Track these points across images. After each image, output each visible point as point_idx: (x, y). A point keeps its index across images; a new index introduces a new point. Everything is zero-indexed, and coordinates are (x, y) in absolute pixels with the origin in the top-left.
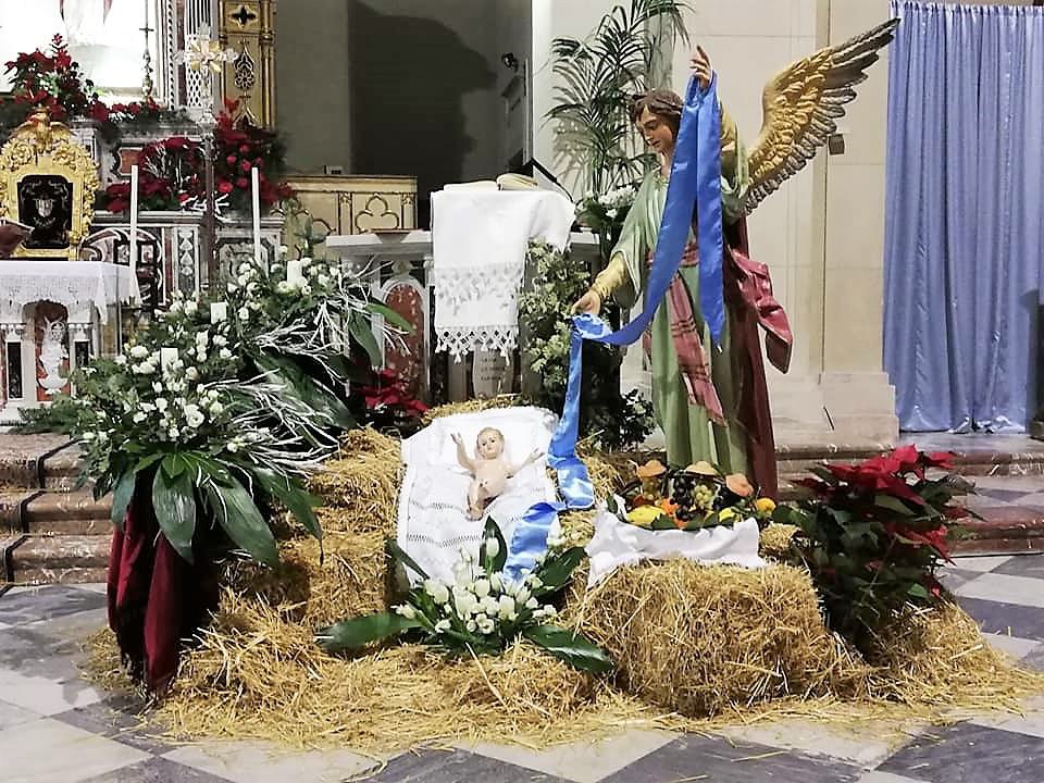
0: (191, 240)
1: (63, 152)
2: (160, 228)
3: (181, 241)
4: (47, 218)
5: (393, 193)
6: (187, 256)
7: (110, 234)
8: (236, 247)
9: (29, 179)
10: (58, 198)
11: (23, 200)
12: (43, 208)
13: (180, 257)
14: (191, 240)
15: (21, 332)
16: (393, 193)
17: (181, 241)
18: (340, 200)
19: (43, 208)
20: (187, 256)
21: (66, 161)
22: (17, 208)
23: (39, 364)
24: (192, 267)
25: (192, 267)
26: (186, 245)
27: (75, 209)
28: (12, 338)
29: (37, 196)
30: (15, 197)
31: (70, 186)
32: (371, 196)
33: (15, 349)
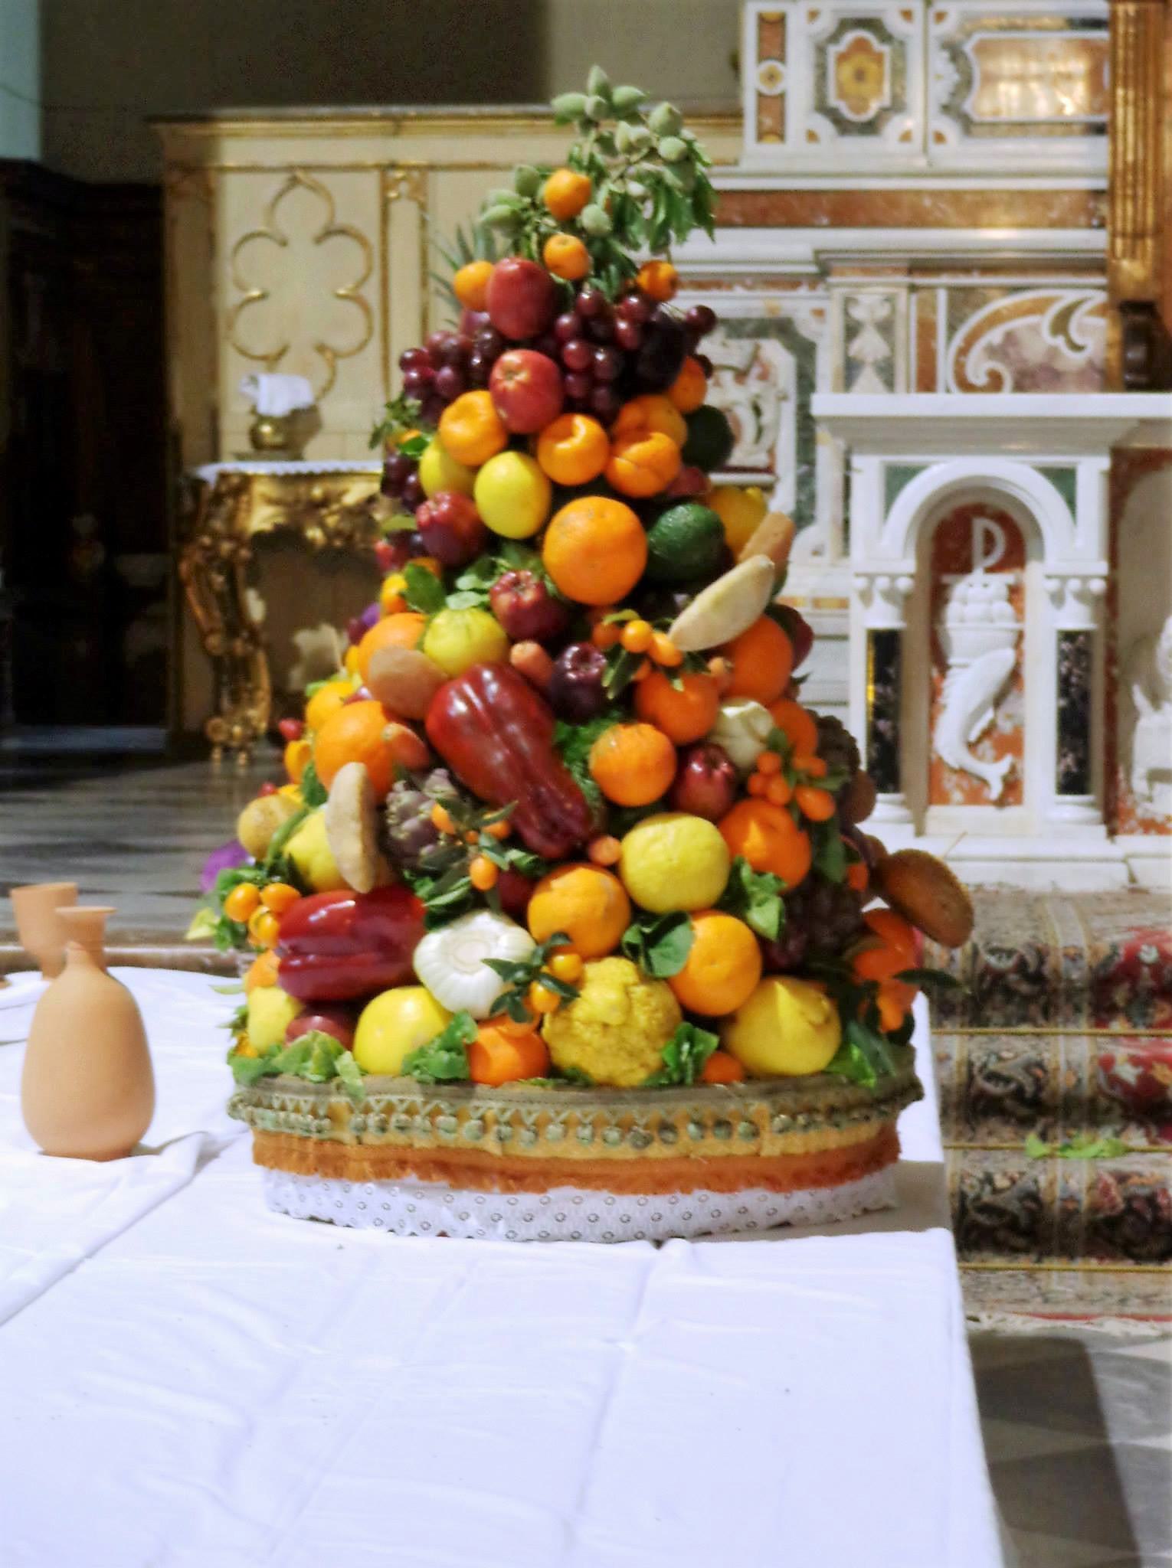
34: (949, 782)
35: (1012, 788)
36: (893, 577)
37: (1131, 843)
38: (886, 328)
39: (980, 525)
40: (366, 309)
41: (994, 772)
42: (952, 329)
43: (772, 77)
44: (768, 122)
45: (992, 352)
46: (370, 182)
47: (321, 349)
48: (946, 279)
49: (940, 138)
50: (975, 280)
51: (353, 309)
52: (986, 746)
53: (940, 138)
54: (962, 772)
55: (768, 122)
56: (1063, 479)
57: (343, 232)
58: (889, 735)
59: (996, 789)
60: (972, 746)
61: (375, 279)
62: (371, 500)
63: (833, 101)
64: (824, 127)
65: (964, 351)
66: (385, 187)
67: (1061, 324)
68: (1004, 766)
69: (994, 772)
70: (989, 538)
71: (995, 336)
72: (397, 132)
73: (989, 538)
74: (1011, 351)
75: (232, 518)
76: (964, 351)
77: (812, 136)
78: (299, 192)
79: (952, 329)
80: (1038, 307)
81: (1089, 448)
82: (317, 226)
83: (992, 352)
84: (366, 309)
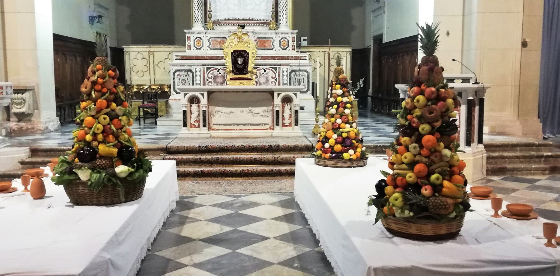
0: (287, 71)
1: (246, 42)
2: (276, 68)
3: (283, 72)
4: (240, 65)
5: (343, 52)
6: (285, 77)
7: (260, 70)
8: (298, 73)
9: (235, 51)
10: (245, 57)
11: (233, 58)
12: (240, 61)
13: (283, 77)
14: (287, 71)
15: (279, 107)
16: (343, 52)
17: (283, 72)
18: (325, 54)
19: (240, 61)
20: (285, 77)
21: (247, 45)
22: (231, 61)
23: (283, 116)
24: (287, 80)
25: (287, 80)
26: (285, 73)
27: (250, 61)
28: (277, 109)
29: (238, 57)
30: (230, 57)
31: (248, 53)
32: (335, 53)
33: (277, 112)
34: (192, 125)
35: (199, 126)
37: (210, 131)
38: (200, 71)
39: (195, 99)
40: (147, 67)
41: (197, 124)
42: (207, 72)
43: (189, 43)
44: (189, 48)
45: (211, 74)
47: (142, 71)
48: (206, 66)
49: (207, 50)
50: (209, 66)
52: (196, 122)
53: (207, 50)
54: (193, 124)
55: (189, 48)
56: (202, 95)
59: (197, 126)
60: (195, 122)
61: (148, 63)
62: (147, 88)
63: (196, 46)
64: (195, 49)
65: (208, 74)
66: (149, 54)
67: (218, 71)
68: (198, 124)
69: (197, 124)
70: (196, 100)
71: (211, 72)
72: (150, 47)
73: (196, 100)
75: (132, 90)
76: (208, 74)
77: (193, 50)
79: (207, 72)
80: (216, 69)
81: (205, 92)
83: (211, 74)
84: (147, 67)
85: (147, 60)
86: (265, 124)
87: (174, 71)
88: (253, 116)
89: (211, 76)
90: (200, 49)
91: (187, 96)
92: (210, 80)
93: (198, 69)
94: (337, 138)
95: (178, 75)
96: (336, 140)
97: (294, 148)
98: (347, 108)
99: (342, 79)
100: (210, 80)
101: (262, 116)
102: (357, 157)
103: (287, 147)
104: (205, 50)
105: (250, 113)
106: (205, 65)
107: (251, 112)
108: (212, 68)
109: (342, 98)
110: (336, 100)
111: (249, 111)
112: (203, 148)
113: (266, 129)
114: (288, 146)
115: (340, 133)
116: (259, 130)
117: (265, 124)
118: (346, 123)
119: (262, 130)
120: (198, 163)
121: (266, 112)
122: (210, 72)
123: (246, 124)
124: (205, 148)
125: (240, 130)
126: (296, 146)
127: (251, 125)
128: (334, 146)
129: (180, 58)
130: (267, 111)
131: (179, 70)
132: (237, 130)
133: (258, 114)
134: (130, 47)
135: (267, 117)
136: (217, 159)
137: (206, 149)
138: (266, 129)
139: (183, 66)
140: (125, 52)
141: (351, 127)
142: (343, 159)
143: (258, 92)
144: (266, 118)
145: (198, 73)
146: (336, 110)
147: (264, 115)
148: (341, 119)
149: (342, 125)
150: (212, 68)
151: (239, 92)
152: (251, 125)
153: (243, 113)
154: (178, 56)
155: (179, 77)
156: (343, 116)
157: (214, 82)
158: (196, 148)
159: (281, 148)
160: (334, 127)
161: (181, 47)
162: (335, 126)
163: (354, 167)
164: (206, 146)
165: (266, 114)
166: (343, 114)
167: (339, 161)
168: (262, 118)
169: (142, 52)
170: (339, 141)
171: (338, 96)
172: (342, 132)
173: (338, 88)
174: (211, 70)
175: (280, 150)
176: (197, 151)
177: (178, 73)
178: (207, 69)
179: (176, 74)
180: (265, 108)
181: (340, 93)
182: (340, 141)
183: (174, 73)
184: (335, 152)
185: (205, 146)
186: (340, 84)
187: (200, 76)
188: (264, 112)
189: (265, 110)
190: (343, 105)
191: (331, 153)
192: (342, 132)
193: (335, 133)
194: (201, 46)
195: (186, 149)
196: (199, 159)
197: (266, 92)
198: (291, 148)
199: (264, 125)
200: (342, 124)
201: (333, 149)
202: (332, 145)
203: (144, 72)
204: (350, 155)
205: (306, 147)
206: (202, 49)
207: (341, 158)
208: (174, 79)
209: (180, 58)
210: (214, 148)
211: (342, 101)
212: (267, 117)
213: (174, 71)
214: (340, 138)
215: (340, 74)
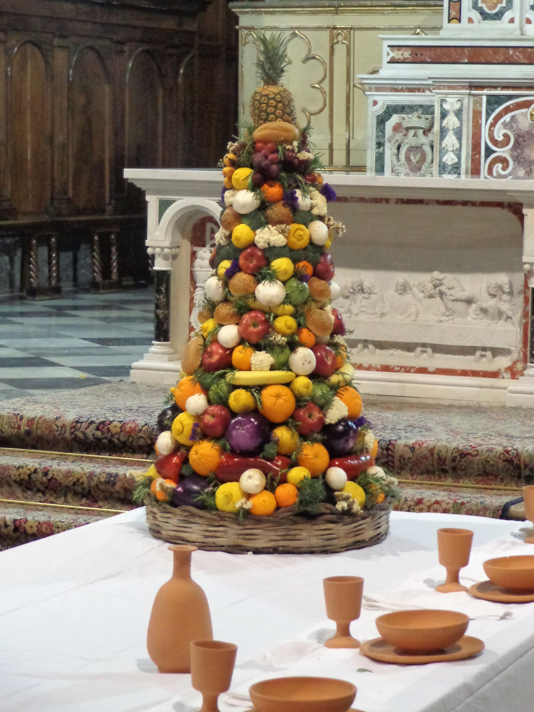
36: (162, 248)
38: (459, 113)
40: (323, 93)
42: (488, 115)
44: (453, 13)
46: (326, 35)
48: (485, 92)
51: (318, 93)
53: (529, 21)
55: (453, 13)
57: (314, 58)
58: (161, 316)
61: (327, 80)
63: (480, 4)
64: (476, 15)
65: (493, 125)
66: (332, 38)
71: (507, 118)
72: (337, 13)
74: (514, 125)
76: (493, 125)
77: (470, 20)
78: (296, 39)
79: (488, 115)
82: (303, 55)
83: (505, 125)
85: (323, 63)
86: (496, 352)
87: (379, 109)
88: (450, 312)
89: (506, 136)
90: (498, 16)
91: (171, 212)
92: (500, 152)
93: (452, 104)
94: (205, 412)
95: (397, 128)
96: (198, 417)
97: (454, 460)
98: (272, 277)
99: (265, 141)
100: (500, 152)
101: (484, 311)
102: (278, 508)
103: (425, 452)
104: (517, 20)
105: (438, 299)
106: (482, 87)
107: (441, 294)
108: (511, 97)
109: (254, 229)
110: (229, 237)
111: (430, 286)
112: (91, 431)
113: (495, 375)
114: (431, 451)
115: (225, 388)
116: (464, 373)
117: (496, 352)
118: (258, 347)
119: (475, 374)
120: (39, 491)
121: (505, 297)
122: (497, 119)
123: (417, 345)
124: (97, 429)
125: (386, 368)
126: (463, 454)
127: (437, 349)
128: (188, 449)
129: (407, 54)
130: (511, 293)
131: (401, 109)
132: (369, 368)
133: (469, 302)
134: (260, 13)
135: (508, 318)
136: (107, 482)
137: (98, 433)
138: (495, 375)
139: (419, 90)
140: (243, 33)
141: (285, 366)
142: (214, 508)
143: (465, 203)
144: (502, 322)
145: (452, 121)
146: (226, 285)
147: (491, 310)
148: (237, 324)
149: (238, 355)
150: (511, 97)
151: (387, 201)
152: (437, 349)
153: (408, 297)
154: (399, 47)
155: (399, 136)
156: (250, 310)
157: (516, 159)
158: (64, 426)
159: (402, 456)
160: (207, 361)
161: (414, 12)
162: (211, 355)
163: (257, 551)
164: (103, 423)
165: (505, 307)
166: (250, 302)
167: (193, 515)
168: (485, 322)
169: (307, 33)
170: (207, 426)
171: (239, 218)
172: (235, 387)
173: (237, 180)
174: (507, 110)
175: (397, 463)
176: (64, 439)
177: (395, 119)
178: (489, 103)
179: (390, 125)
180: (502, 278)
181: (244, 206)
182: (213, 426)
183: (381, 121)
184: (196, 477)
185: (99, 421)
186: (251, 167)
187: (458, 134)
188: (494, 296)
189: (500, 288)
190: (253, 263)
191: (180, 479)
192: (235, 387)
193: (206, 390)
194: (504, 4)
195: (24, 428)
196: (40, 474)
197: (500, 205)
198: (441, 460)
199: (489, 354)
200: (240, 347)
201: (185, 461)
202: (183, 440)
203: (311, 114)
204: (248, 496)
205: (510, 461)
206: (507, 16)
207: (202, 506)
208: (380, 145)
209: (407, 54)
210: (129, 434)
211: (253, 245)
212: (508, 318)
213: (381, 112)
214: (215, 409)
215: (266, 120)
